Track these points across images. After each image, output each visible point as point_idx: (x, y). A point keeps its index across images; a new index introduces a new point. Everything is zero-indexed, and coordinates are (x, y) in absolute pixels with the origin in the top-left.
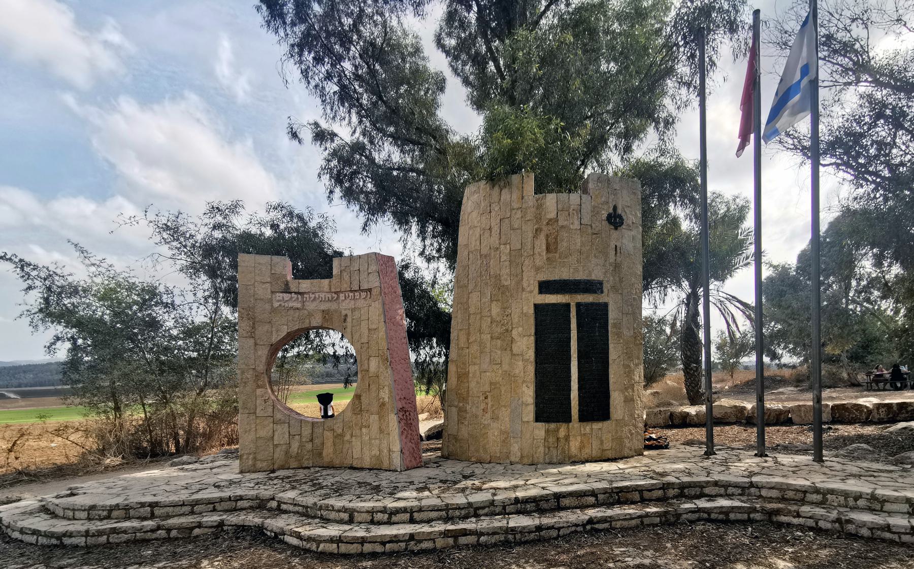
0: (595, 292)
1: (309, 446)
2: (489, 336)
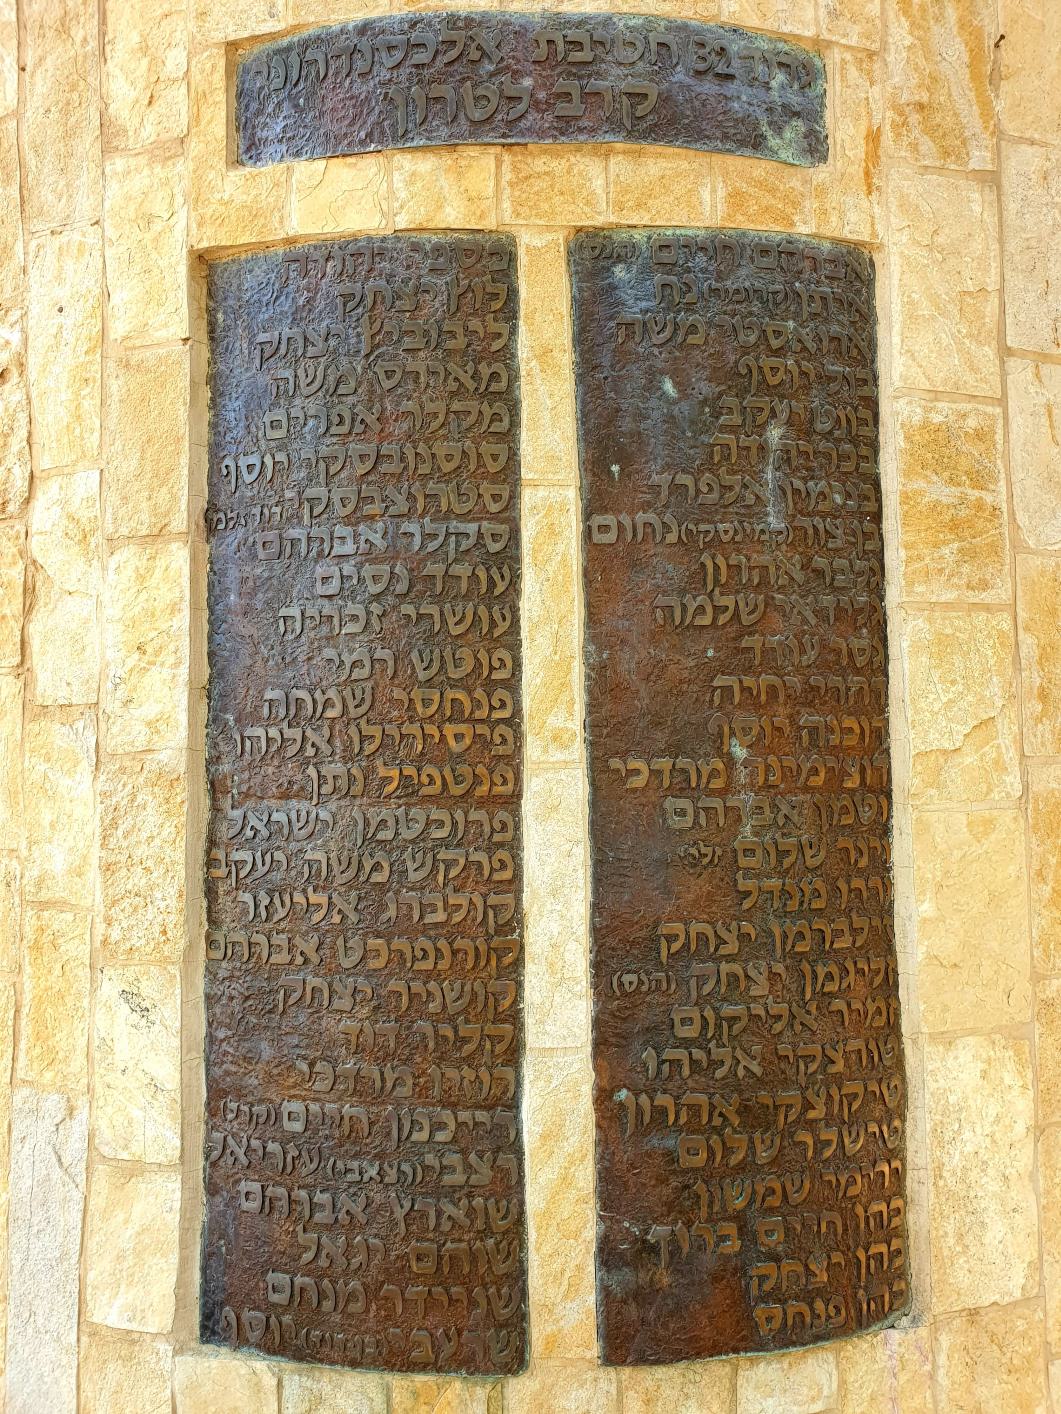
0: (755, 143)
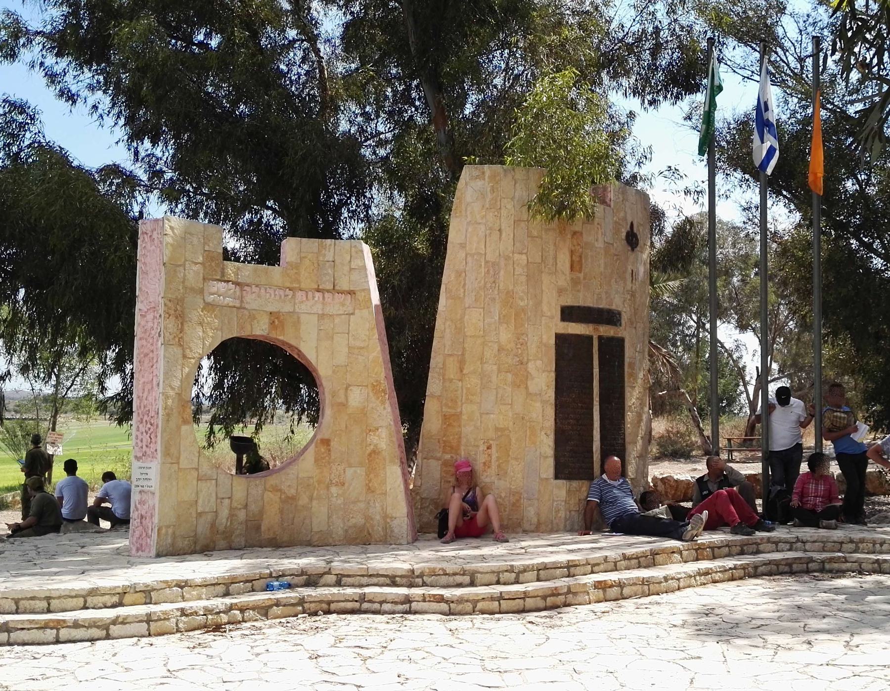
2: (495, 367)
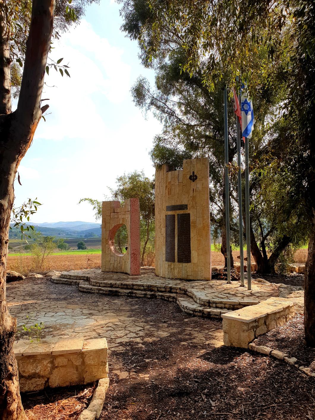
0: (184, 209)
1: (119, 265)
